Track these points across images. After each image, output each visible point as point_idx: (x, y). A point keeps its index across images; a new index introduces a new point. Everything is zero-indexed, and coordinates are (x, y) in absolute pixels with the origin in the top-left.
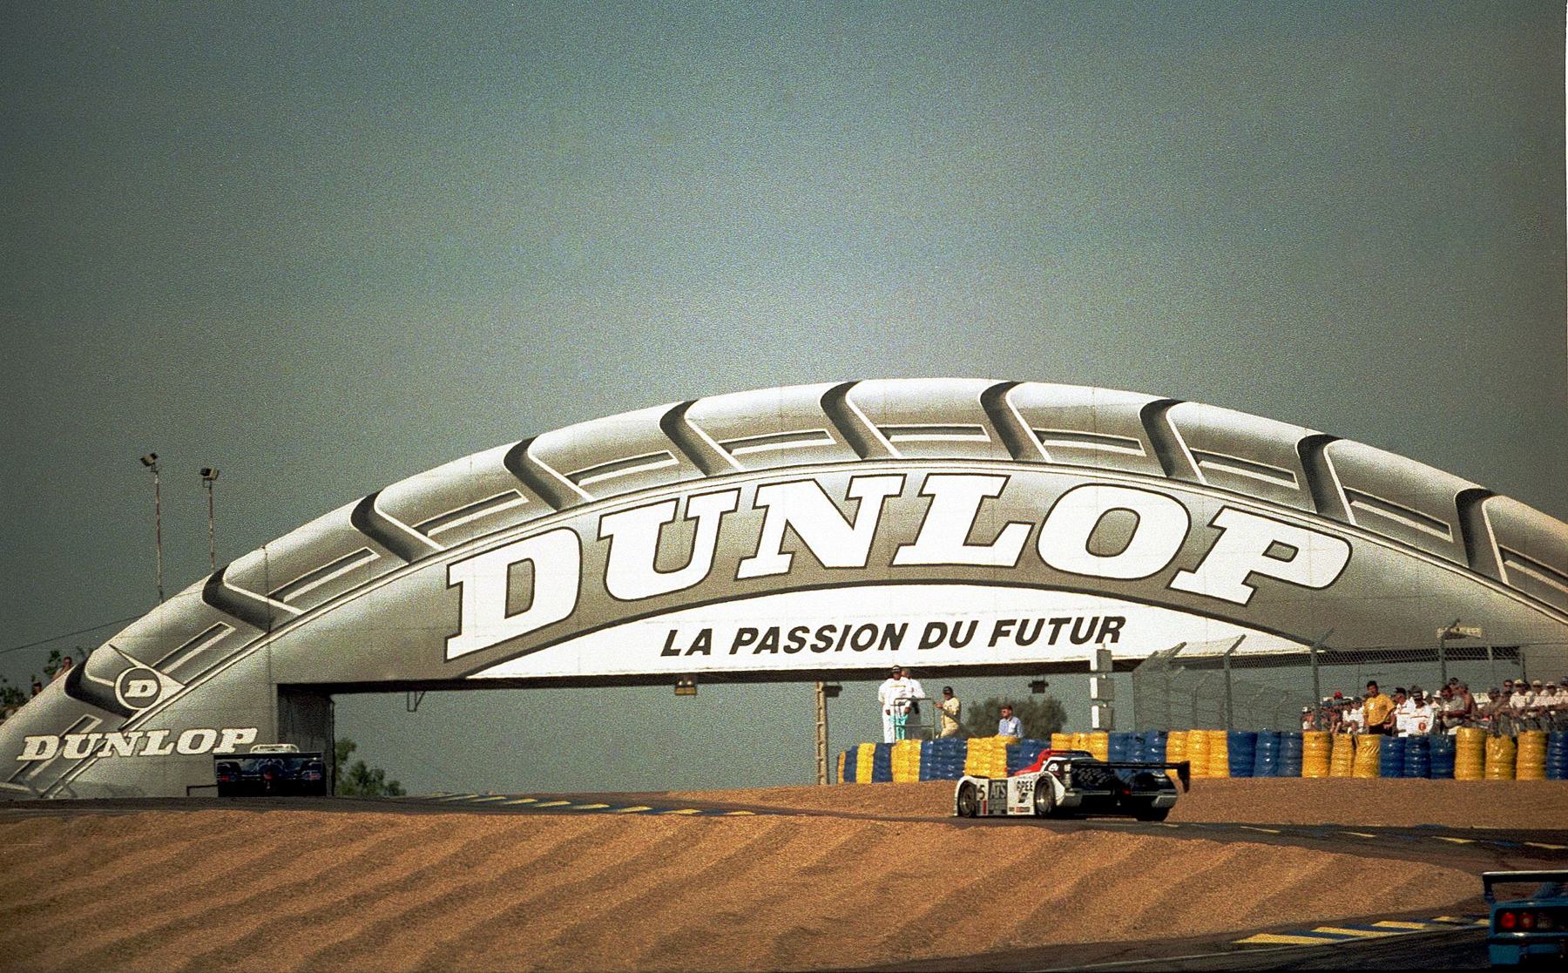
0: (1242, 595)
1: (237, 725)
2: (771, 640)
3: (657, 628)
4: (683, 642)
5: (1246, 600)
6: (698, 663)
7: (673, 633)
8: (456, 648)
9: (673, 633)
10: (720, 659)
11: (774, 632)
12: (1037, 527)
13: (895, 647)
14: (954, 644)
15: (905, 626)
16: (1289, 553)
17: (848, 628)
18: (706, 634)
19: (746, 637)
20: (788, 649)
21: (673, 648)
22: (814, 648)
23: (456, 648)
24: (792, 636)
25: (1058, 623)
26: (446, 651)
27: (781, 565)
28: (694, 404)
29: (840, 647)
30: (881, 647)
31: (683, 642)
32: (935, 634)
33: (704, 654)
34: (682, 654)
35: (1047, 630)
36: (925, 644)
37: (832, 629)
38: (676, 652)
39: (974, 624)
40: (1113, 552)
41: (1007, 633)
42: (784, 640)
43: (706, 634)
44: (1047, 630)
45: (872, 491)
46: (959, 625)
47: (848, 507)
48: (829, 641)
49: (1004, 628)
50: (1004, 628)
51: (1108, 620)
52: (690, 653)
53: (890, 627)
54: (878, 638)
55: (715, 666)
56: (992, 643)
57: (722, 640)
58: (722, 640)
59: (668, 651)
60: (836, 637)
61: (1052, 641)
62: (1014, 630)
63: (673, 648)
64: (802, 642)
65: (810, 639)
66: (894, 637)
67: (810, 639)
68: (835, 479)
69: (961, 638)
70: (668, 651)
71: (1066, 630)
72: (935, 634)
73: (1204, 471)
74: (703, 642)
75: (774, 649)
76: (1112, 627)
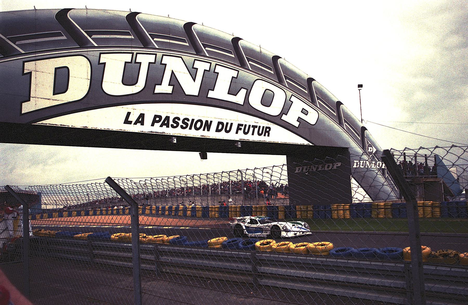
0: (297, 124)
1: (6, 142)
2: (166, 122)
3: (122, 111)
4: (133, 118)
5: (23, 107)
6: (137, 128)
7: (129, 114)
8: (27, 108)
9: (129, 114)
10: (147, 128)
11: (167, 118)
12: (249, 91)
13: (208, 130)
14: (227, 132)
15: (211, 122)
16: (306, 113)
17: (193, 120)
18: (142, 116)
19: (157, 119)
20: (172, 126)
21: (129, 120)
22: (182, 127)
23: (27, 108)
24: (174, 121)
25: (254, 127)
26: (295, 126)
27: (169, 90)
28: (196, 24)
29: (190, 128)
30: (204, 130)
31: (133, 118)
32: (220, 127)
33: (167, 127)
34: (133, 123)
35: (251, 129)
36: (218, 130)
37: (188, 120)
38: (130, 123)
39: (232, 124)
40: (264, 104)
41: (241, 129)
42: (171, 122)
43: (142, 116)
44: (251, 129)
45: (202, 66)
46: (227, 124)
47: (193, 72)
48: (187, 125)
49: (240, 127)
50: (240, 127)
51: (267, 128)
52: (135, 123)
53: (207, 121)
54: (161, 121)
55: (94, 127)
56: (237, 133)
57: (148, 120)
58: (148, 120)
59: (127, 121)
60: (189, 123)
61: (253, 134)
62: (243, 128)
63: (129, 120)
64: (178, 124)
65: (180, 123)
66: (208, 125)
67: (180, 123)
68: (189, 59)
69: (228, 129)
70: (127, 121)
71: (256, 130)
72: (220, 127)
73: (20, 46)
74: (141, 119)
75: (168, 126)
76: (267, 131)
